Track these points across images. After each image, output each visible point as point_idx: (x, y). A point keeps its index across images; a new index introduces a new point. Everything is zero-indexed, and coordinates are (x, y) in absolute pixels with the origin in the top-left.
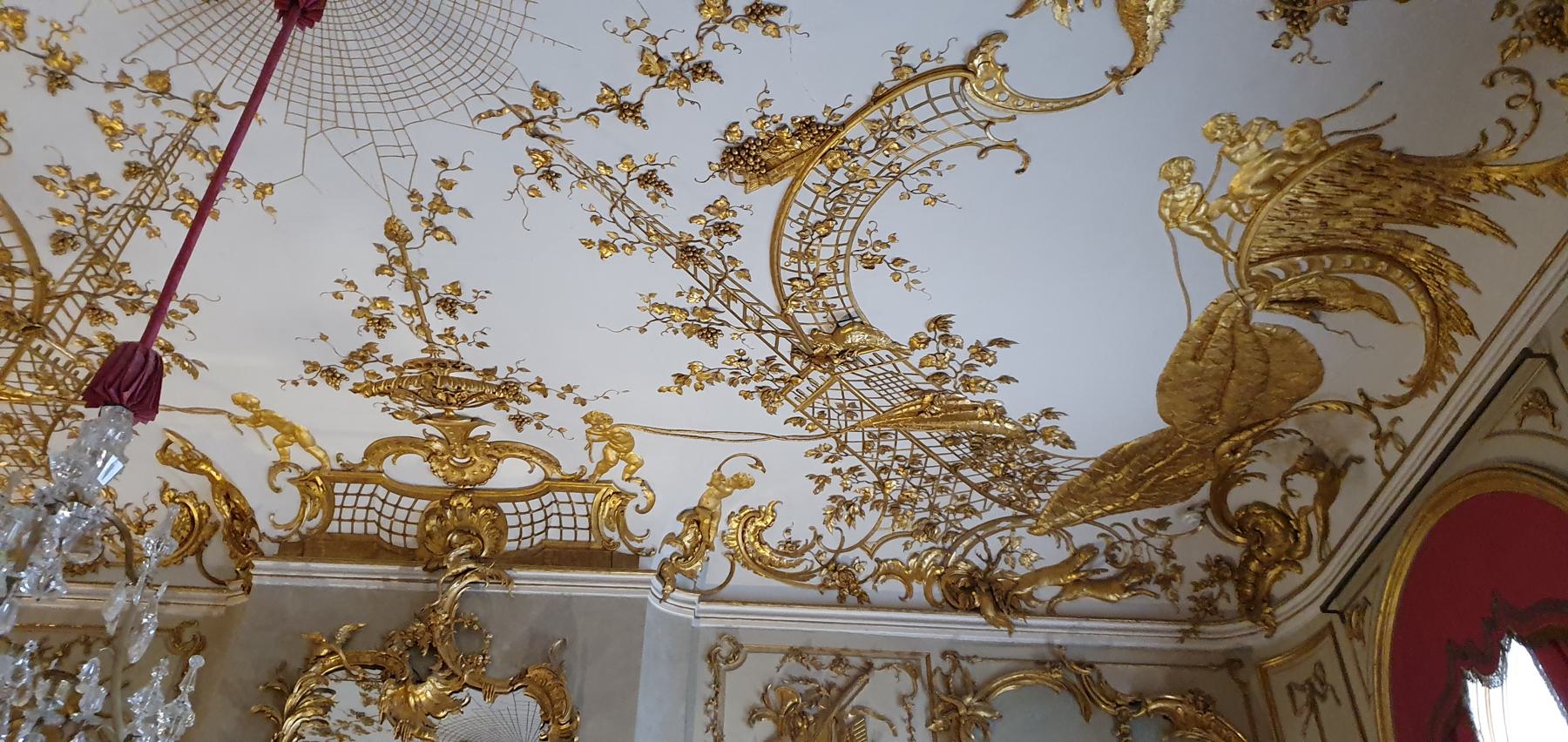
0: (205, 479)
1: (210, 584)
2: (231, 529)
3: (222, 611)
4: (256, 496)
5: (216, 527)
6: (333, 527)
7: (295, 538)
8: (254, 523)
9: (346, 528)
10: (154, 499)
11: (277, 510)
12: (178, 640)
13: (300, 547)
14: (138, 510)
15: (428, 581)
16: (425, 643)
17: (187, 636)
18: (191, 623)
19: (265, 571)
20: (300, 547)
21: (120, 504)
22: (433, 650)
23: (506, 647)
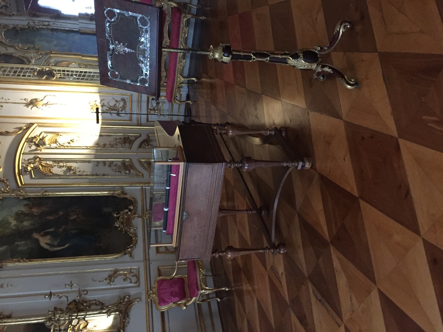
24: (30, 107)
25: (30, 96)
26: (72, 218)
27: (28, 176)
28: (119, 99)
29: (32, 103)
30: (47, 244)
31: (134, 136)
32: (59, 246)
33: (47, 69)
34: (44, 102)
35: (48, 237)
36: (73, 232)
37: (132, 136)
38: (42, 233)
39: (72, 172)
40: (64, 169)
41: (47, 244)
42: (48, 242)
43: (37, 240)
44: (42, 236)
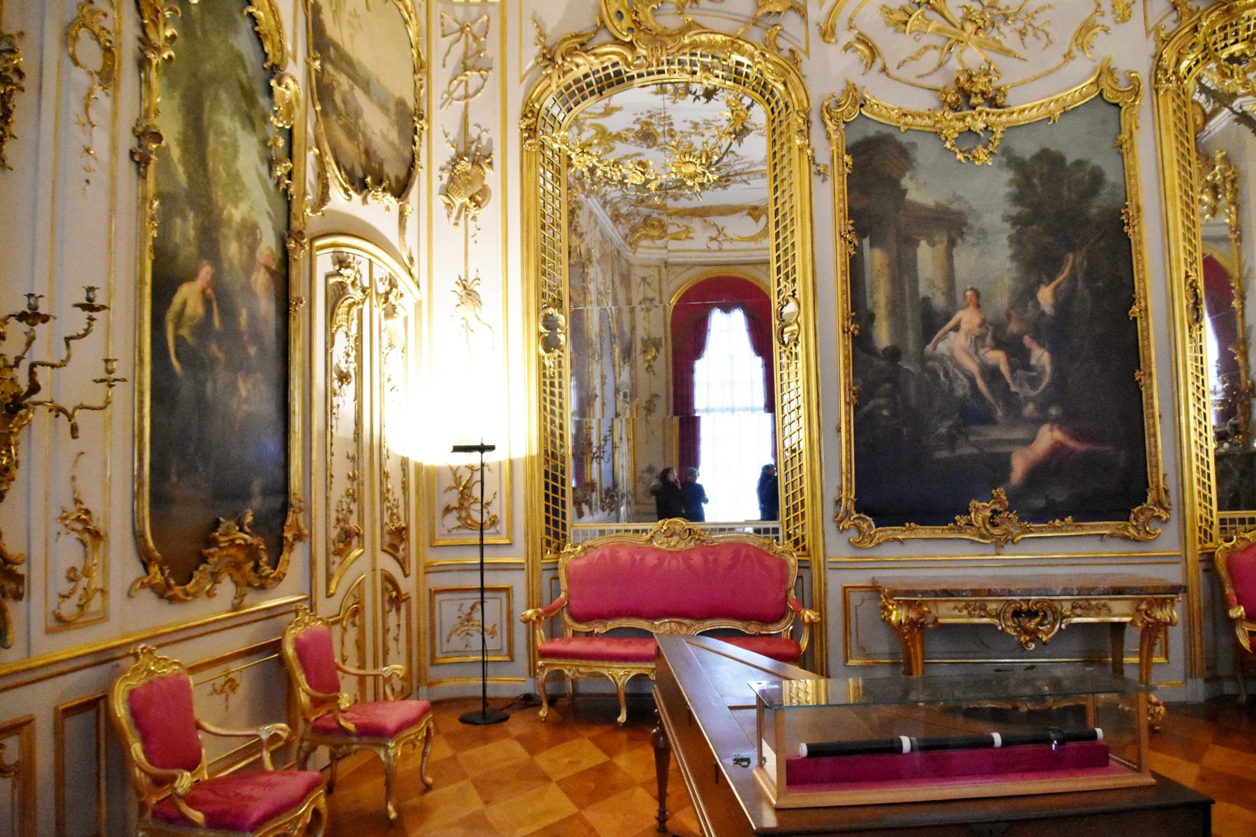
24: (460, 289)
25: (488, 289)
26: (241, 384)
27: (331, 268)
28: (493, 510)
29: (469, 292)
30: (184, 304)
31: (407, 556)
32: (179, 340)
33: (562, 337)
34: (473, 323)
35: (200, 310)
36: (209, 386)
37: (406, 549)
38: (209, 291)
39: (336, 384)
40: (343, 367)
41: (184, 304)
42: (189, 311)
43: (192, 277)
44: (203, 292)
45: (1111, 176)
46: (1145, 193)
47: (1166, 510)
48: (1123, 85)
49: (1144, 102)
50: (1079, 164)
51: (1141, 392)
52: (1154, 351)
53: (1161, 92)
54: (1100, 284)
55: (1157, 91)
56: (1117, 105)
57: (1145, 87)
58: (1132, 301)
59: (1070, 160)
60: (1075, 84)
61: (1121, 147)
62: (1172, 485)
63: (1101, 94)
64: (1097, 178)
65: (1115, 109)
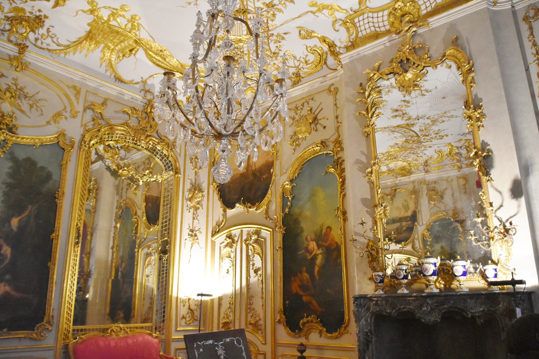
0: (316, 38)
1: (333, 71)
2: (330, 50)
3: (339, 78)
4: (332, 36)
5: (327, 54)
6: (360, 35)
7: (350, 44)
8: (336, 46)
9: (364, 33)
10: (306, 52)
11: (341, 38)
12: (330, 91)
13: (353, 45)
14: (303, 58)
15: (399, 38)
16: (404, 59)
17: (332, 89)
18: (332, 85)
19: (345, 58)
20: (353, 45)
21: (298, 59)
22: (408, 60)
23: (435, 48)
45: (55, 177)
46: (67, 188)
47: (51, 325)
48: (68, 142)
49: (74, 151)
50: (42, 168)
51: (49, 272)
52: (58, 255)
53: (82, 150)
54: (41, 221)
55: (80, 148)
56: (64, 149)
57: (76, 146)
58: (53, 231)
59: (39, 165)
60: (48, 135)
61: (61, 166)
62: (55, 314)
63: (58, 143)
64: (49, 176)
65: (62, 150)
